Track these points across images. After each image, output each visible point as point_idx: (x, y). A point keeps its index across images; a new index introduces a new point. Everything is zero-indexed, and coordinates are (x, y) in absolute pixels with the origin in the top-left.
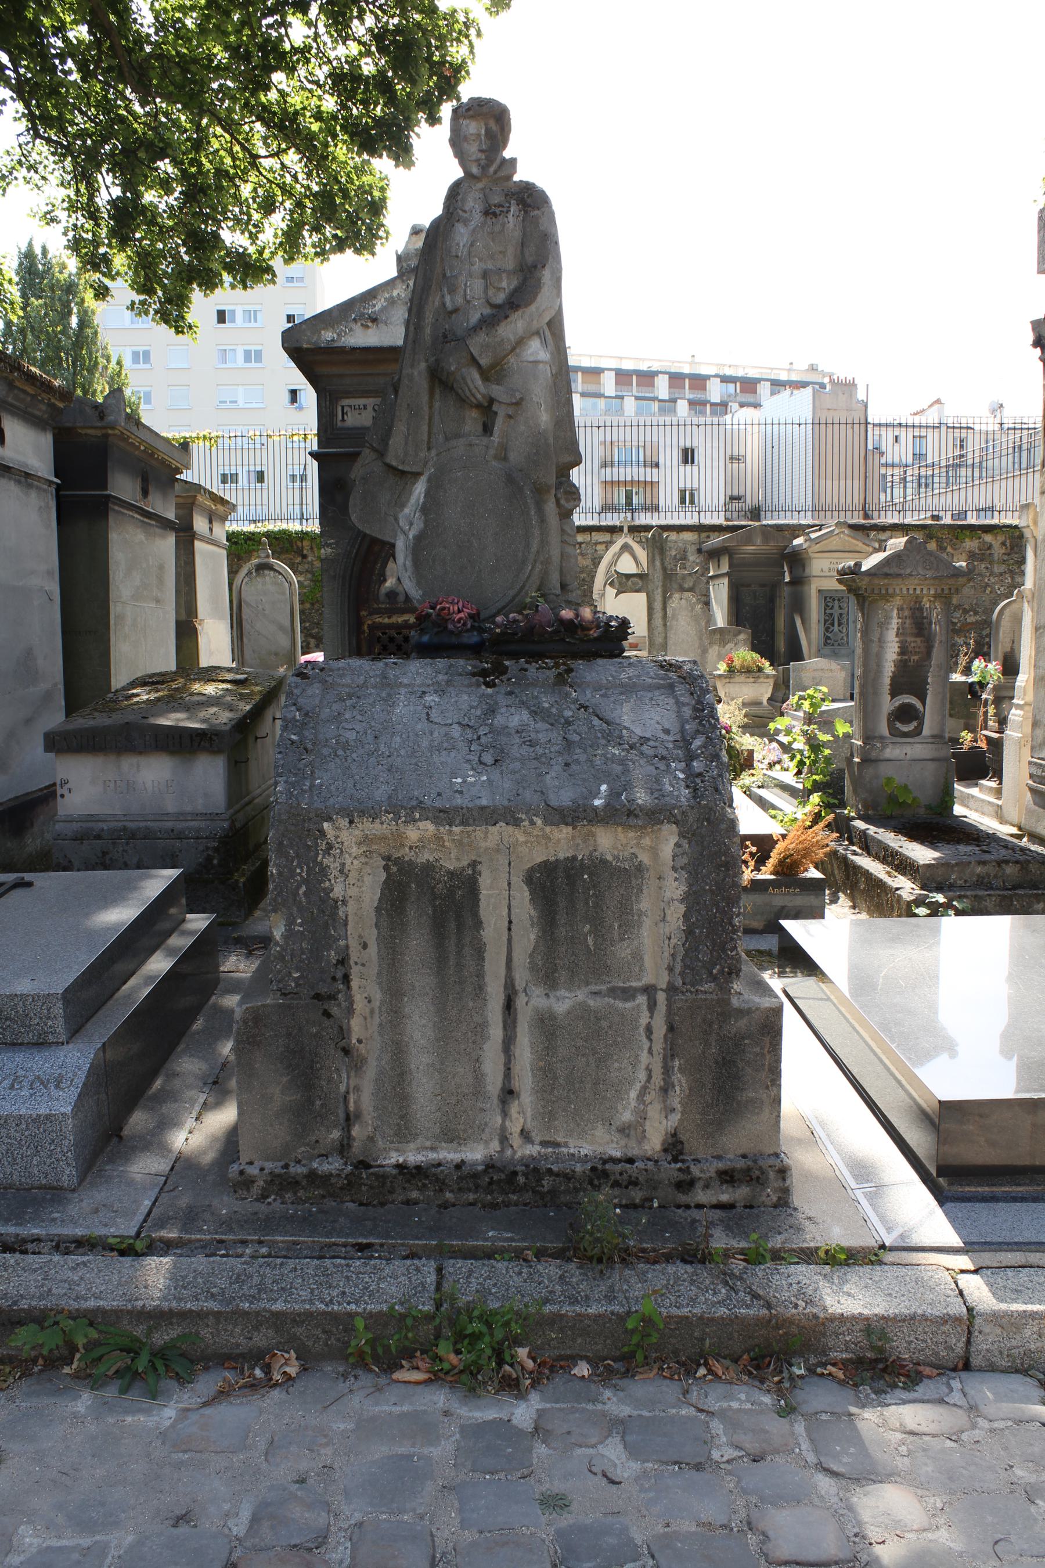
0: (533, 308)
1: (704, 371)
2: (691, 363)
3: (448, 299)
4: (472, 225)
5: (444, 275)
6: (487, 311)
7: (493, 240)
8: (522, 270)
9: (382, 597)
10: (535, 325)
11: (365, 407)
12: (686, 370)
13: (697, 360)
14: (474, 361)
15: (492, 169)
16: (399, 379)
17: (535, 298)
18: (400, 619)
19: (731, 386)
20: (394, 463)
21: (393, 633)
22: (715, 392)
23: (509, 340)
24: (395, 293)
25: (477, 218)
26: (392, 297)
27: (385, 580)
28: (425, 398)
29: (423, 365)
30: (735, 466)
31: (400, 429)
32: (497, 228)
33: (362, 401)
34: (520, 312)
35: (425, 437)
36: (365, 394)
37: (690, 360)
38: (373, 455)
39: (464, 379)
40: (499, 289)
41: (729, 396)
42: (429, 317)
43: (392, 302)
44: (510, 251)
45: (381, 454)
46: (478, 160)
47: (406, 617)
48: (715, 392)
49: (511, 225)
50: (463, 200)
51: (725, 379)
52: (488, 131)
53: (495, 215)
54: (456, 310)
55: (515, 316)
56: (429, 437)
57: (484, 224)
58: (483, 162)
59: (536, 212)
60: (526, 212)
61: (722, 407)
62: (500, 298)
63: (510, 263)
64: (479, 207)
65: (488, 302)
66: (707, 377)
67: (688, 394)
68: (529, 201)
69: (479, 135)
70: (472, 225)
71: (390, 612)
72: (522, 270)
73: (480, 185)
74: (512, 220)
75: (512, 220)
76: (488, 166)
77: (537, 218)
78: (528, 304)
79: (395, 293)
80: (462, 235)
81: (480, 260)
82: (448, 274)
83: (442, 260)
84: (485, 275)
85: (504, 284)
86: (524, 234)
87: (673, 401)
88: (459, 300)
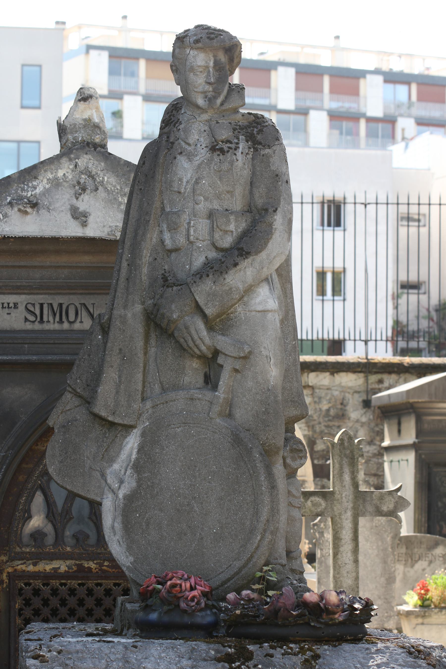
0: (263, 255)
1: (355, 63)
2: (334, 49)
3: (167, 236)
4: (197, 160)
5: (163, 209)
6: (213, 254)
7: (220, 179)
8: (250, 211)
9: (25, 539)
10: (265, 272)
11: (16, 306)
12: (325, 61)
13: (342, 43)
14: (199, 309)
15: (219, 101)
16: (110, 319)
17: (266, 244)
18: (47, 567)
19: (402, 90)
20: (103, 414)
21: (38, 583)
22: (374, 98)
23: (237, 289)
24: (60, 173)
25: (203, 154)
26: (56, 179)
27: (30, 517)
28: (140, 343)
29: (138, 308)
30: (413, 230)
31: (110, 376)
32: (225, 166)
33: (11, 299)
34: (249, 260)
35: (140, 388)
36: (17, 290)
37: (332, 43)
38: (76, 401)
39: (187, 328)
40: (226, 232)
41: (399, 106)
42: (146, 255)
43: (56, 183)
44: (239, 191)
45: (88, 401)
46: (204, 92)
47: (55, 564)
48: (374, 98)
49: (240, 163)
50: (187, 131)
51: (392, 78)
52: (216, 63)
53: (222, 151)
54: (177, 250)
55: (244, 263)
56: (144, 387)
57: (210, 160)
58: (210, 95)
59: (267, 151)
60: (256, 150)
61: (385, 127)
62: (227, 242)
63: (237, 204)
64: (204, 141)
65: (213, 245)
66: (362, 74)
67: (329, 102)
68: (259, 137)
69: (207, 67)
70: (197, 160)
71: (36, 558)
72: (250, 211)
73: (205, 117)
74: (241, 159)
75: (241, 159)
76: (215, 98)
77: (267, 157)
78: (258, 252)
79: (60, 173)
80: (185, 170)
81: (206, 199)
82: (168, 209)
83: (161, 192)
84: (211, 215)
85: (232, 227)
86: (254, 173)
87: (303, 112)
88: (181, 240)
